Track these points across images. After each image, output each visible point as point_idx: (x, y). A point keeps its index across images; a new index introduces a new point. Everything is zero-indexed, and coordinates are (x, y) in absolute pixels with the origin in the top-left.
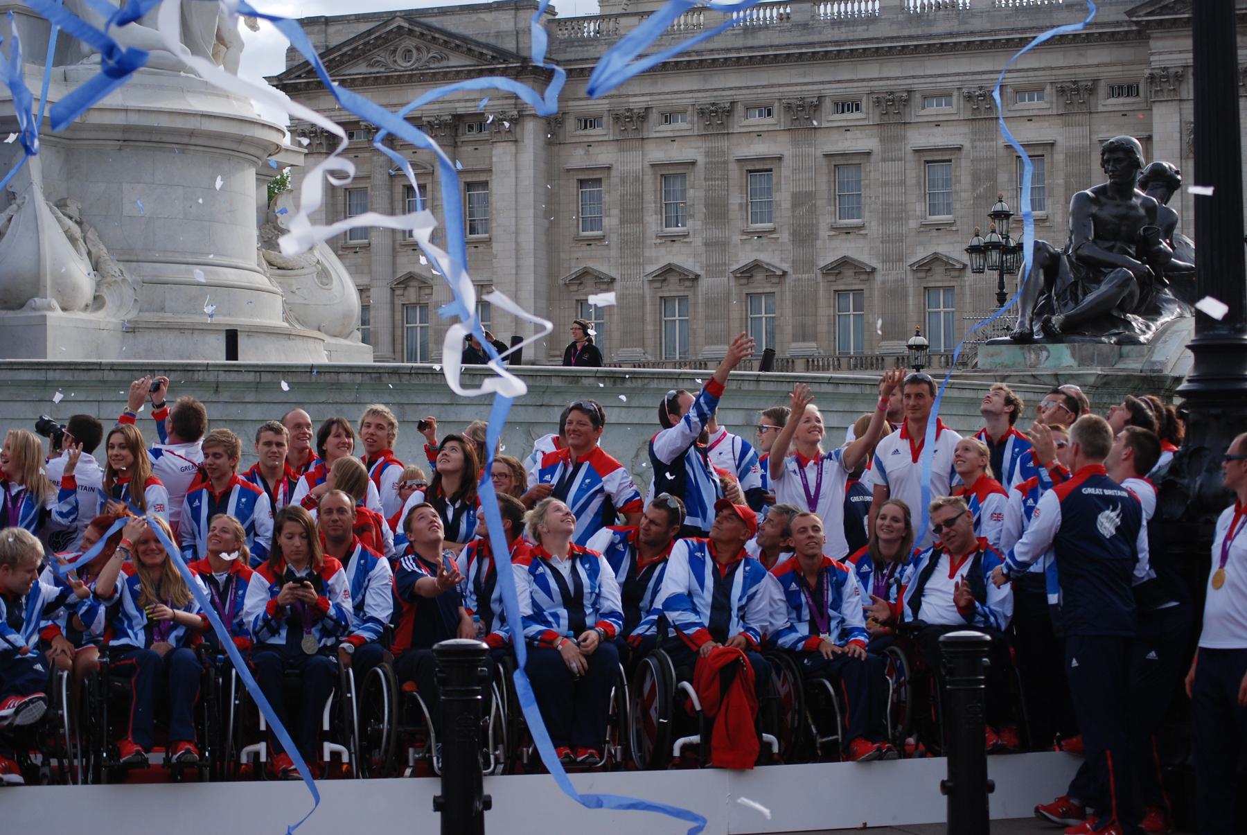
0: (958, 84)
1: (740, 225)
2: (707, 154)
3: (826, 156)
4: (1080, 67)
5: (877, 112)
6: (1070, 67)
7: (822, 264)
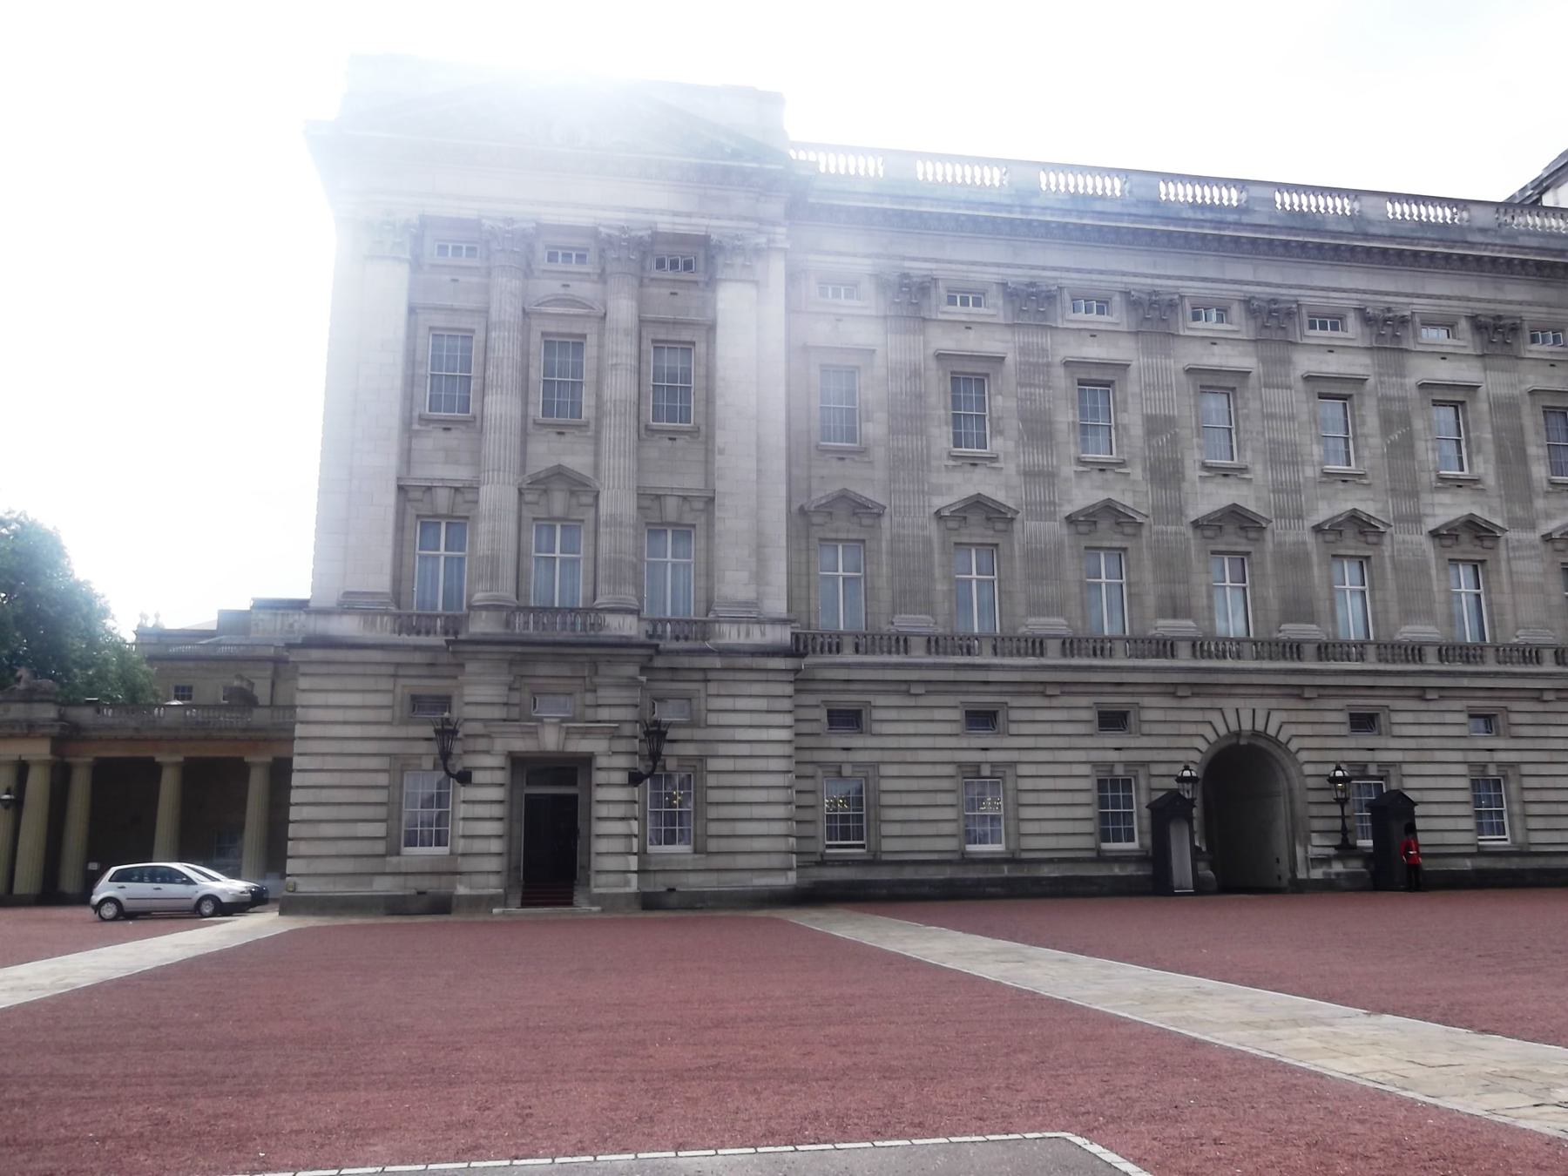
0: (1355, 304)
1: (1073, 451)
2: (1024, 350)
3: (1190, 371)
4: (1500, 302)
5: (1252, 323)
6: (1489, 301)
7: (1193, 514)
